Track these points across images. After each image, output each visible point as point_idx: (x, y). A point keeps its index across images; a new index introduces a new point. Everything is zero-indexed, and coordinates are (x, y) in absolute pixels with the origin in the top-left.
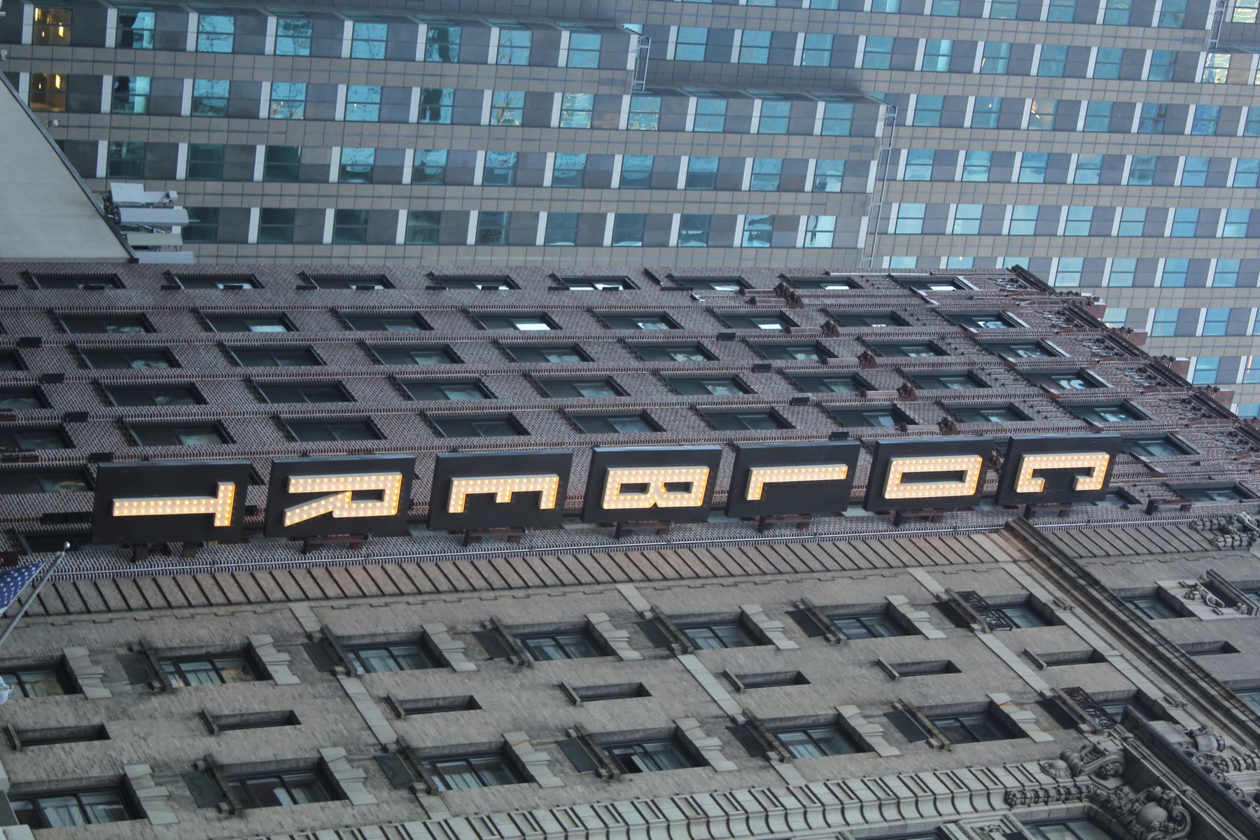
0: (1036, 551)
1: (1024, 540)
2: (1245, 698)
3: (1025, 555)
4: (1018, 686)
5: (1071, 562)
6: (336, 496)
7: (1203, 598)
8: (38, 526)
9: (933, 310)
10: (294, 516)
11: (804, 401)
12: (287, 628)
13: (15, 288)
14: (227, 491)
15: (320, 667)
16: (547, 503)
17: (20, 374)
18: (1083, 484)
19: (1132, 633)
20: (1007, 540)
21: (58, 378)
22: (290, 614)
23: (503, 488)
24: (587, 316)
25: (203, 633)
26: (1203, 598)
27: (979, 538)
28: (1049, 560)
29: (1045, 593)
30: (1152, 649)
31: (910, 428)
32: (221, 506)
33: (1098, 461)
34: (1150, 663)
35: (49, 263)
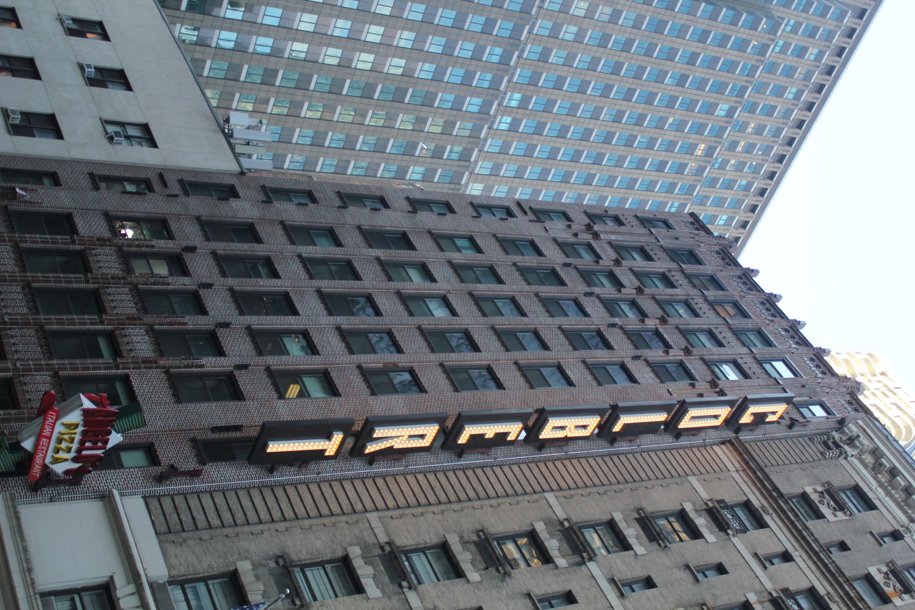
0: (747, 463)
1: (740, 454)
2: (855, 584)
3: (741, 466)
4: (758, 587)
5: (761, 469)
6: (399, 437)
7: (828, 504)
8: (211, 436)
9: (661, 246)
10: (371, 448)
11: (613, 325)
12: (368, 539)
13: (177, 196)
14: (338, 437)
15: (392, 579)
16: (511, 438)
17: (186, 280)
18: (771, 418)
19: (804, 538)
20: (731, 452)
21: (209, 286)
22: (368, 525)
23: (489, 431)
24: (493, 240)
25: (318, 544)
26: (828, 504)
27: (716, 448)
28: (755, 473)
29: (757, 501)
30: (799, 531)
31: (623, 290)
32: (330, 447)
33: (781, 408)
34: (759, 490)
35: (195, 172)
